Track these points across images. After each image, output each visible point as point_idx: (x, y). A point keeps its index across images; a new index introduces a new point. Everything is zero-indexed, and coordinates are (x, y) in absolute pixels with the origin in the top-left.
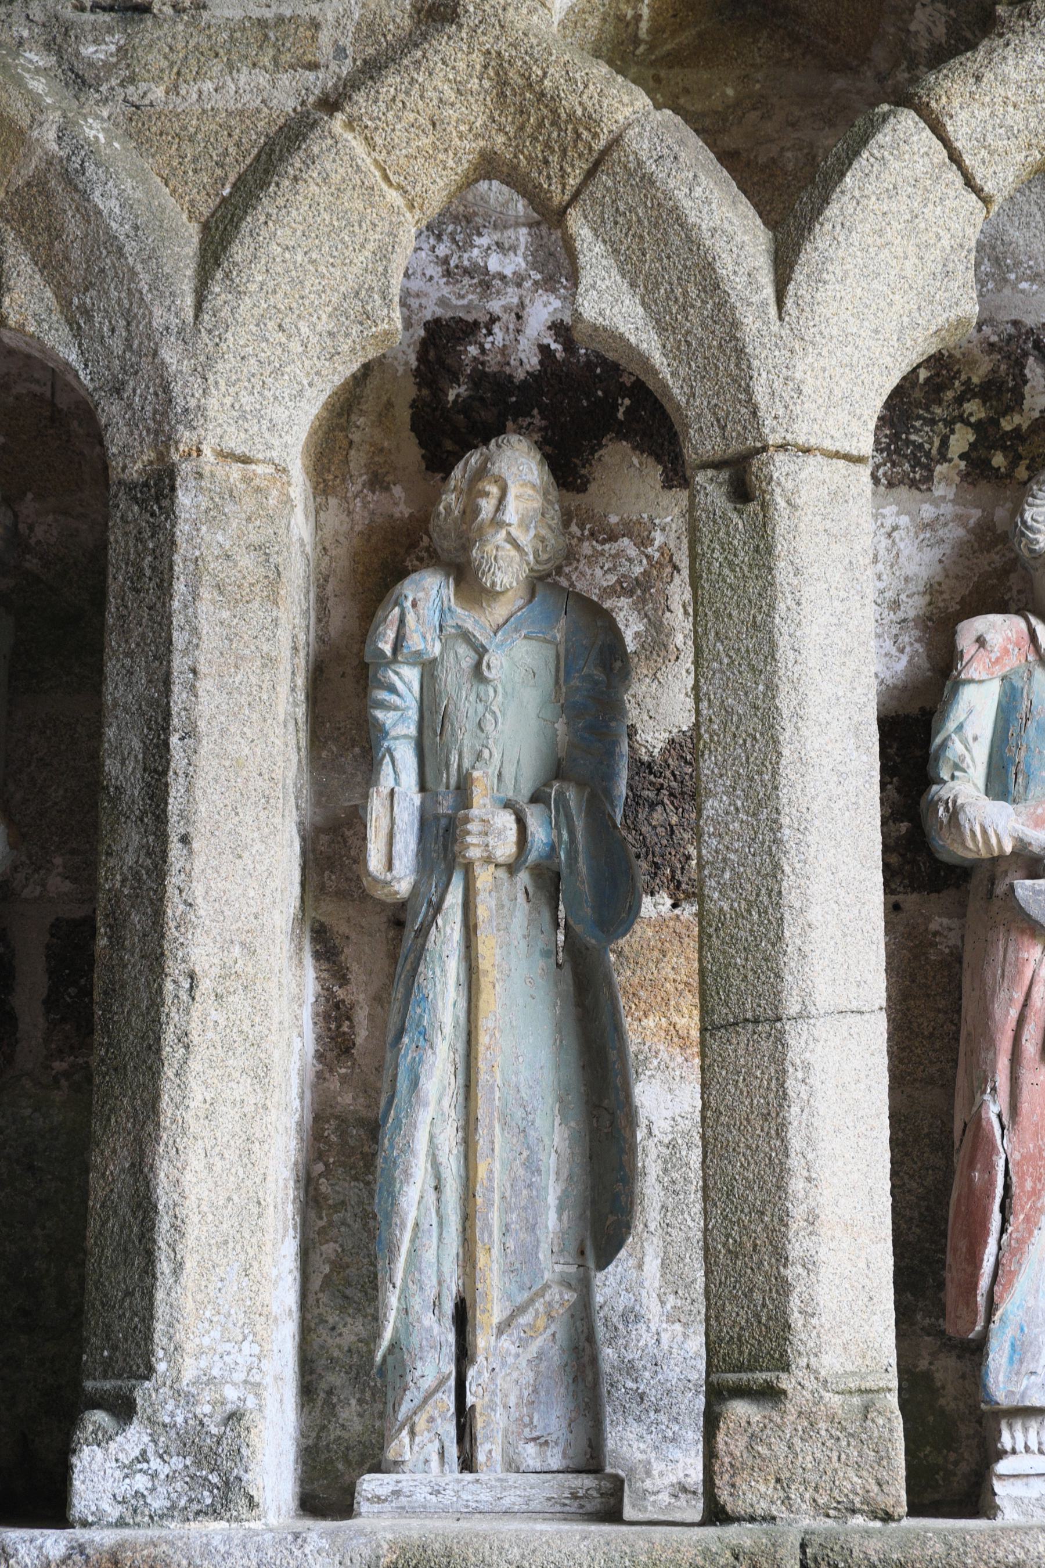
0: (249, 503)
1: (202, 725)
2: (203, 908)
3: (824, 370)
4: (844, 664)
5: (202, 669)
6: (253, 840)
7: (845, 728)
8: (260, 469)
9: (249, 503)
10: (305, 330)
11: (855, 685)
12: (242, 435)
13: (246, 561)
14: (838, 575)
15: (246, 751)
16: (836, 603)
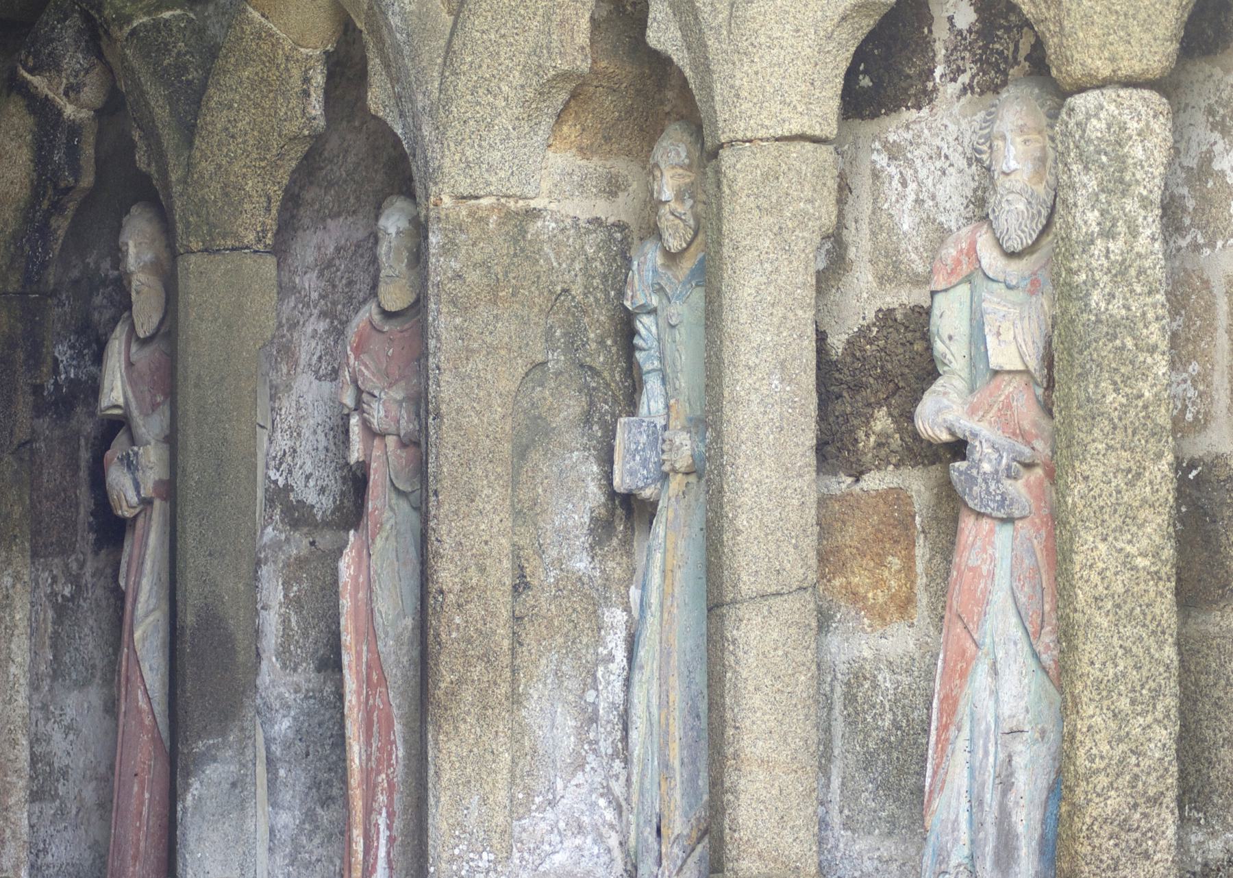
0: (475, 232)
1: (444, 407)
2: (448, 542)
3: (756, 73)
4: (772, 314)
5: (442, 366)
6: (483, 487)
7: (772, 366)
8: (484, 202)
9: (475, 232)
10: (505, 88)
11: (781, 329)
12: (468, 181)
13: (473, 276)
14: (768, 241)
15: (476, 421)
16: (766, 265)
